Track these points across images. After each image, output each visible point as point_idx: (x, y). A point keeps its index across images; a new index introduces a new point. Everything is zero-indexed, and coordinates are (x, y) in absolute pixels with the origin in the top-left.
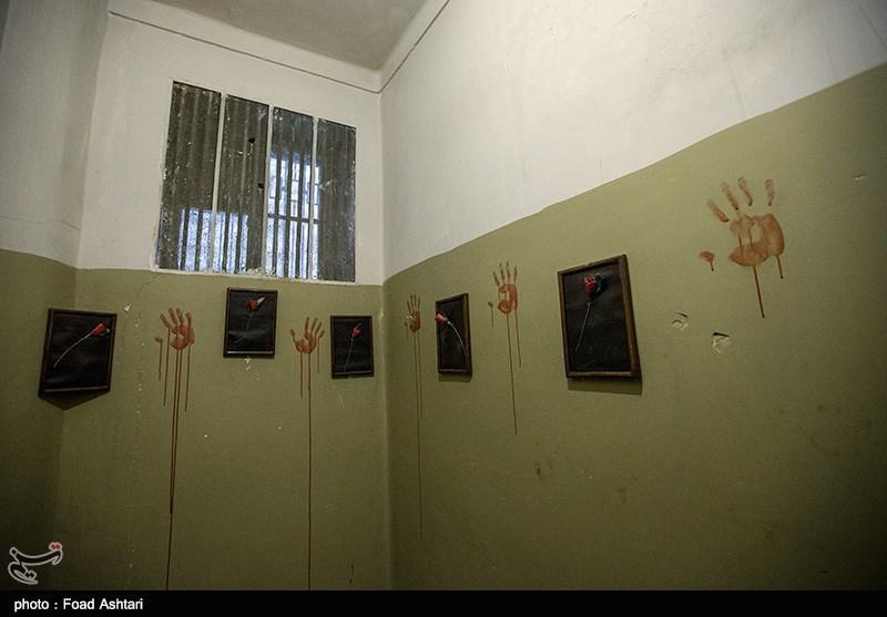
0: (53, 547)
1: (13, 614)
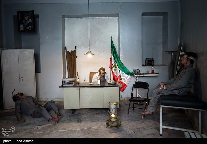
0: (12, 128)
1: (3, 143)
